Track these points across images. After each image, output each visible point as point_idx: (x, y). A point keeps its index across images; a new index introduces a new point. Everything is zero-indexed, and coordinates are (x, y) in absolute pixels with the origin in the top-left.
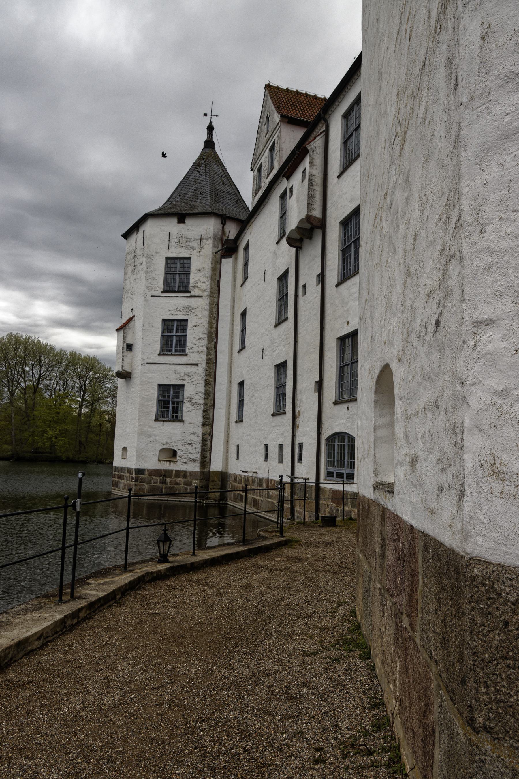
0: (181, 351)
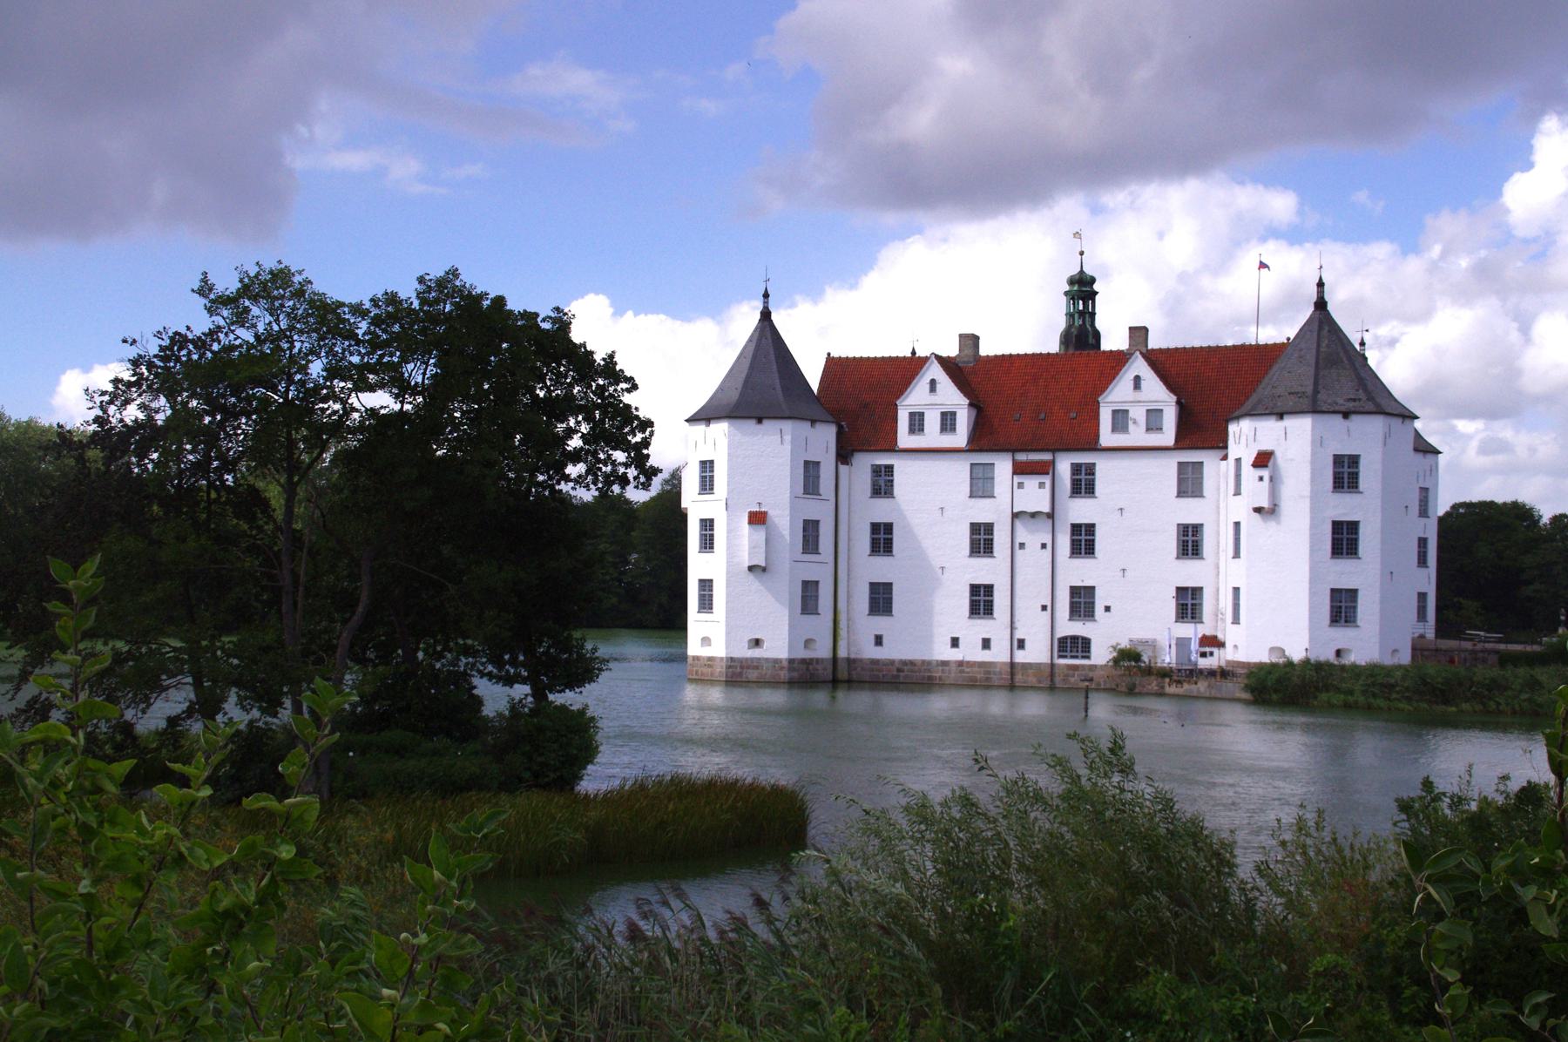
0: (816, 551)
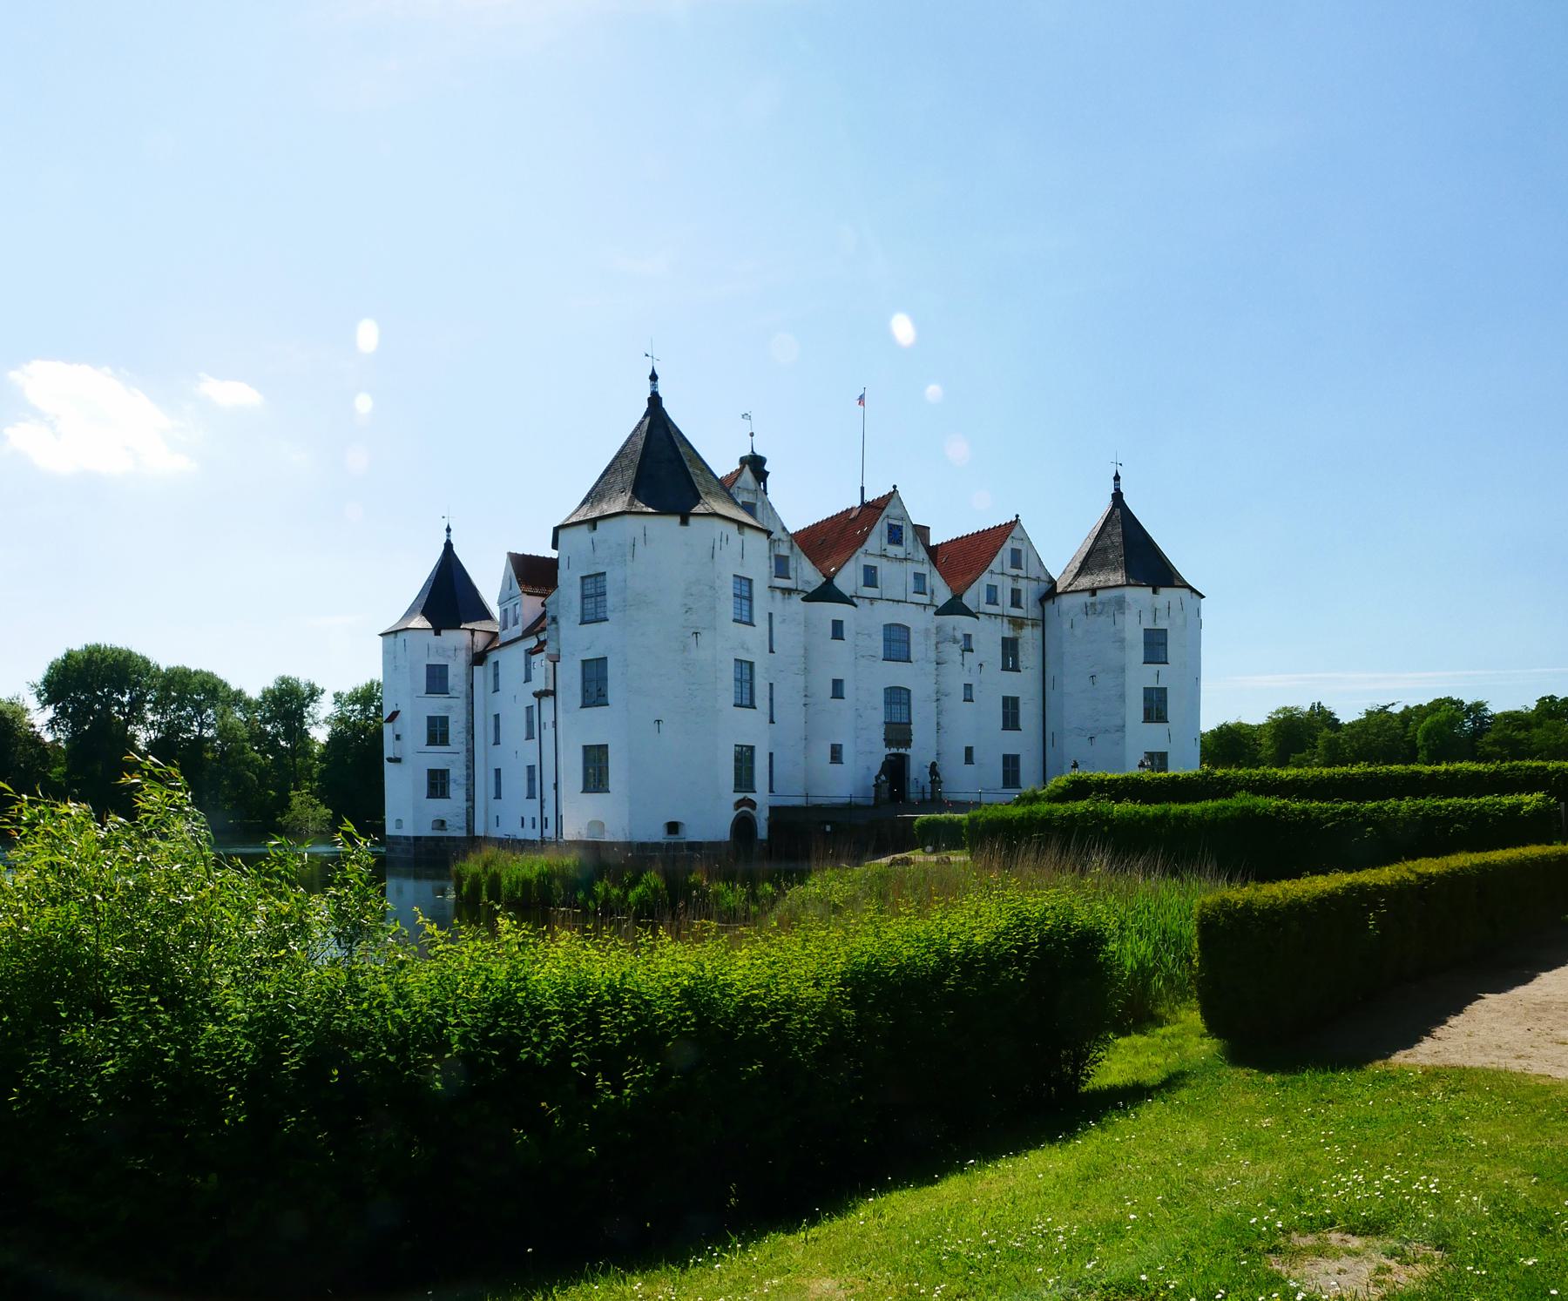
0: (444, 741)
